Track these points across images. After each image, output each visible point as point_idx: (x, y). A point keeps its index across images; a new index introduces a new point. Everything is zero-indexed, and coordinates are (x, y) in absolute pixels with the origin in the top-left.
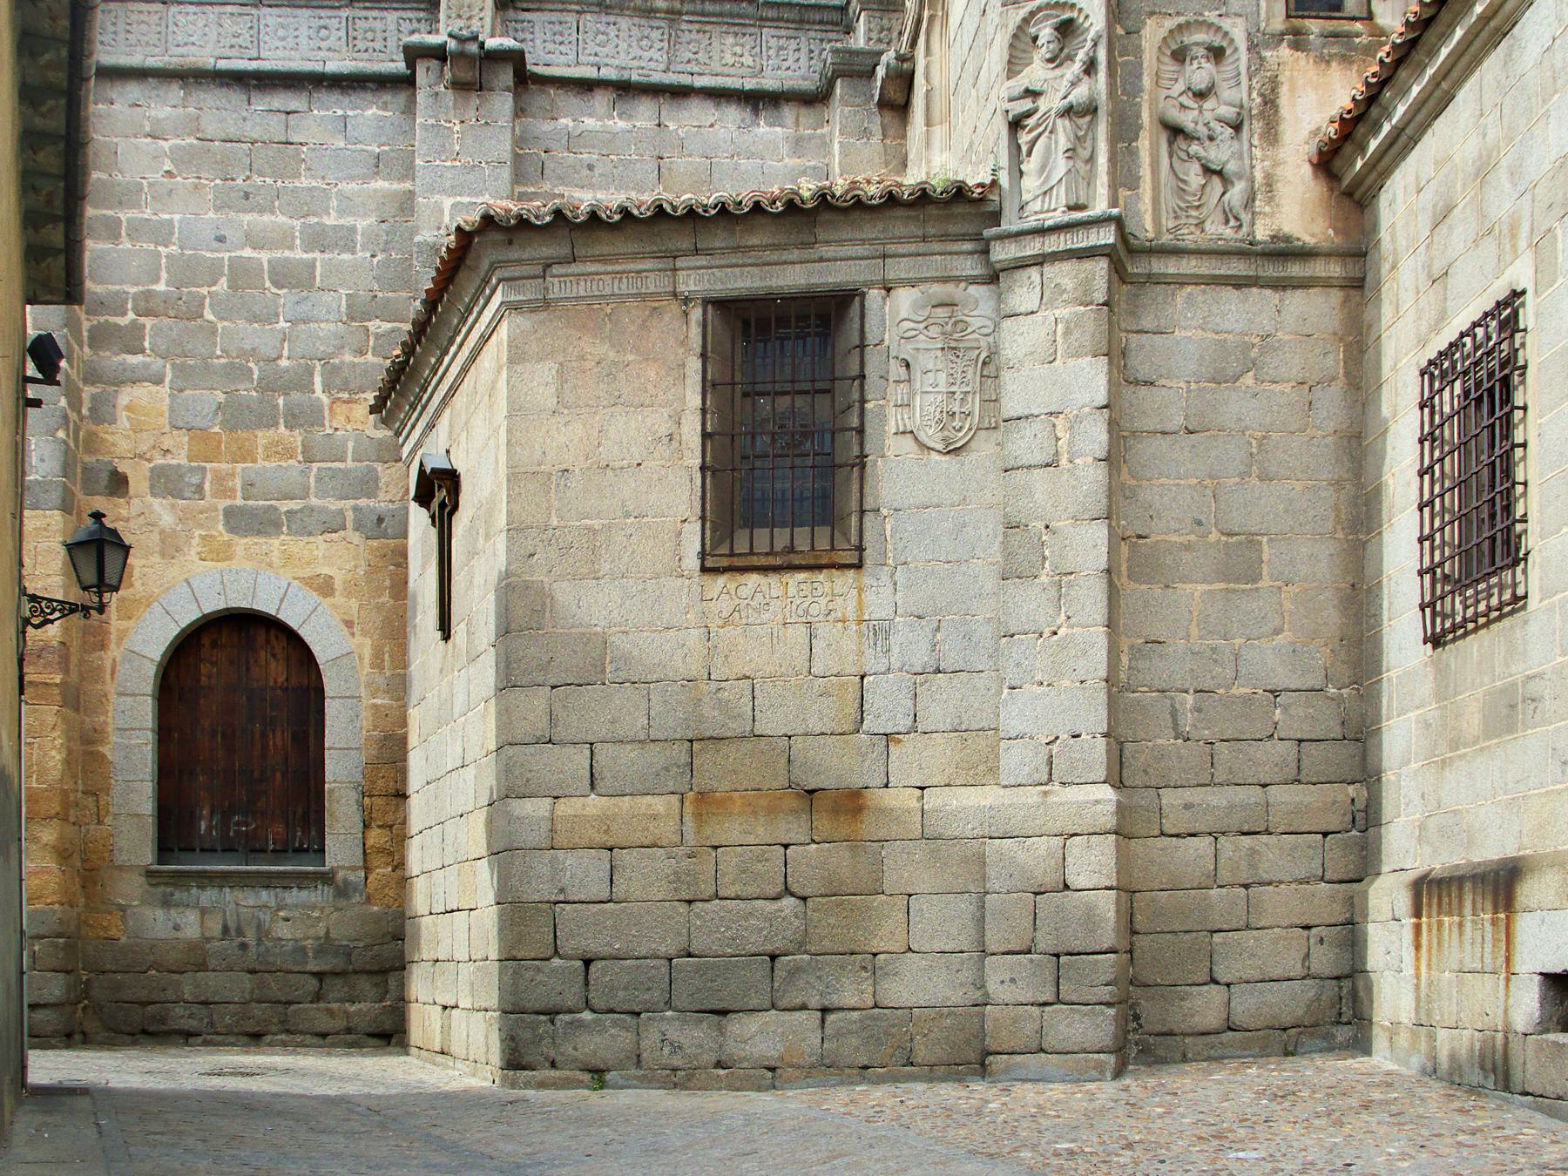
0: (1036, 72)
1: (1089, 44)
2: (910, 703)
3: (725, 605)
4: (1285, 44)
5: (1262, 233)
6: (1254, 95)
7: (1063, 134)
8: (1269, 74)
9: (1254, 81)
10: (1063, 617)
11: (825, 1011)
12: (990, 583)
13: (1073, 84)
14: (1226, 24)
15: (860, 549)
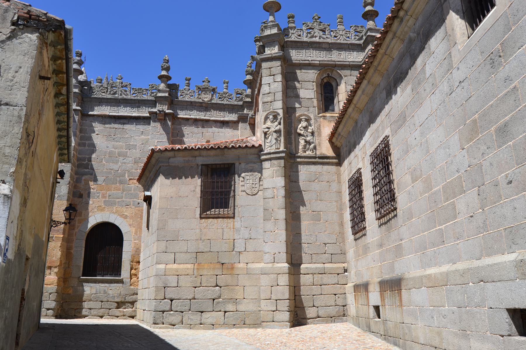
0: (269, 123)
1: (279, 119)
2: (244, 245)
3: (205, 225)
5: (318, 153)
7: (275, 135)
10: (276, 228)
11: (225, 312)
12: (262, 221)
13: (276, 126)
14: (309, 115)
15: (234, 214)
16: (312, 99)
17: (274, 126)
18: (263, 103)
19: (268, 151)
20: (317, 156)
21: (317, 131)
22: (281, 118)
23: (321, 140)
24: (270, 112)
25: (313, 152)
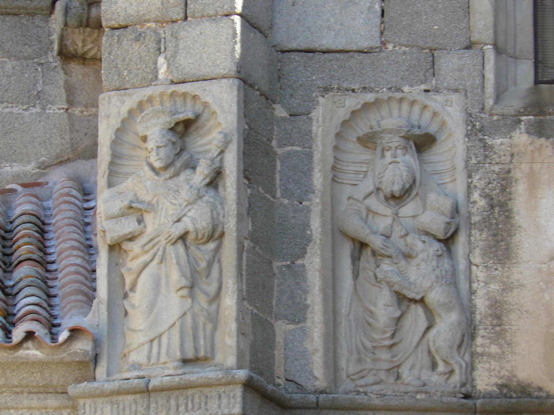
4: (522, 126)
6: (476, 196)
8: (497, 168)
9: (476, 178)
21: (486, 223)
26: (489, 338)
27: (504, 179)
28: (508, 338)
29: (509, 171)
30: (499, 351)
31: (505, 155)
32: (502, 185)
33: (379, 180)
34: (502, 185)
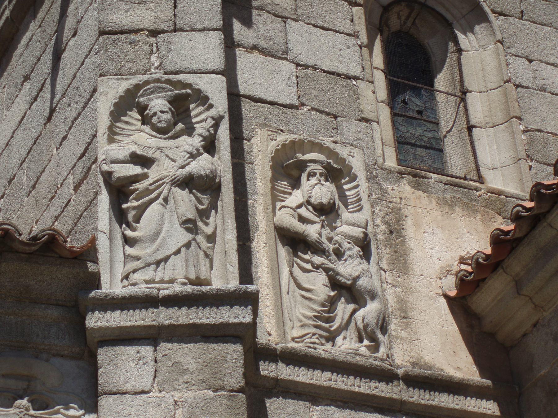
6: (379, 221)
13: (193, 156)
14: (343, 152)
16: (348, 77)
17: (182, 158)
18: (102, 33)
19: (142, 289)
20: (400, 372)
22: (221, 118)
23: (408, 291)
24: (147, 83)
25: (375, 348)
26: (400, 326)
27: (397, 214)
28: (414, 329)
29: (400, 209)
30: (407, 336)
31: (396, 198)
32: (396, 218)
33: (309, 195)
34: (396, 218)
